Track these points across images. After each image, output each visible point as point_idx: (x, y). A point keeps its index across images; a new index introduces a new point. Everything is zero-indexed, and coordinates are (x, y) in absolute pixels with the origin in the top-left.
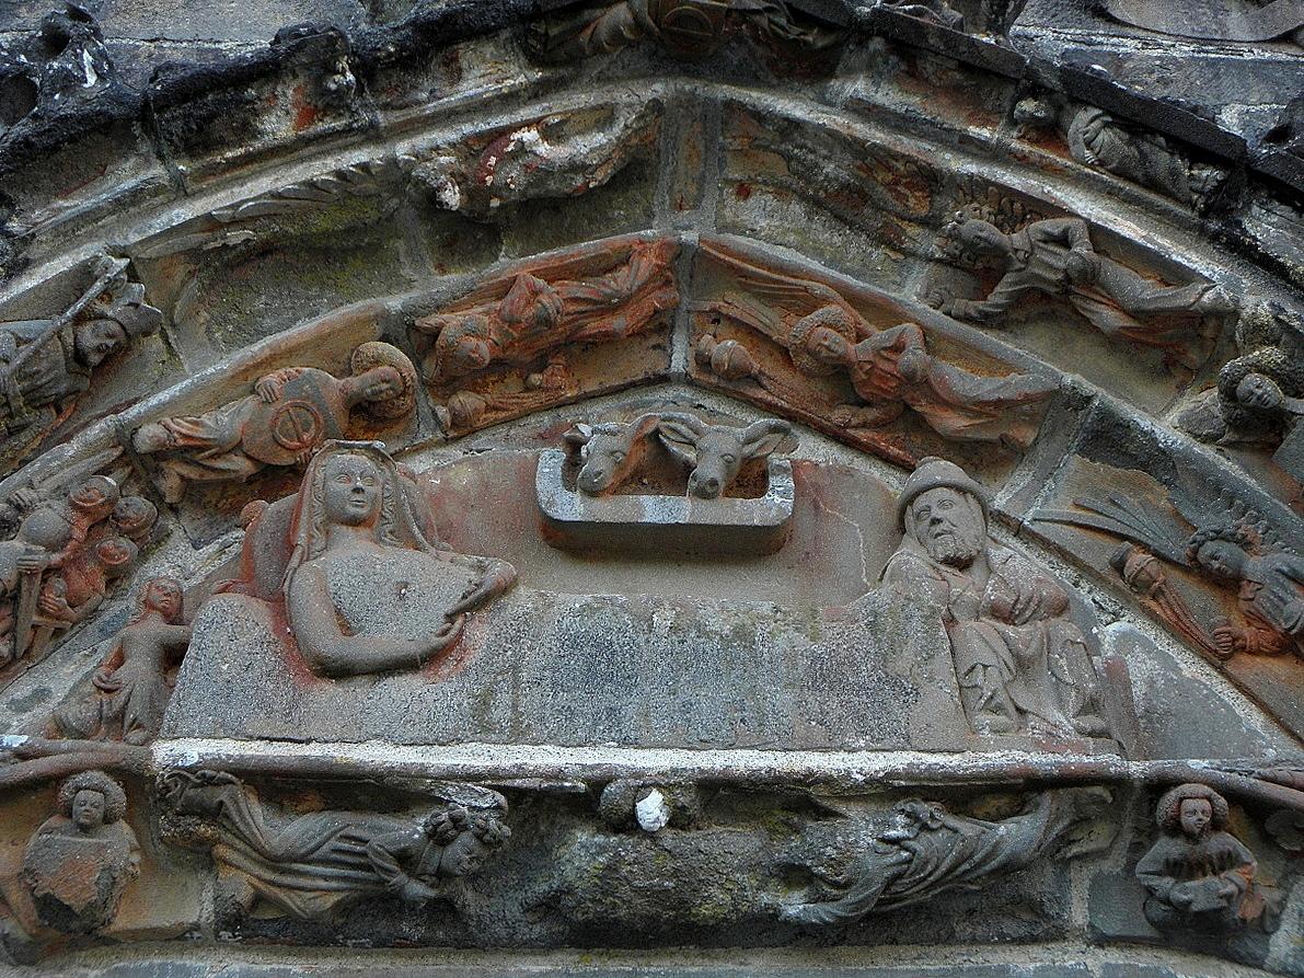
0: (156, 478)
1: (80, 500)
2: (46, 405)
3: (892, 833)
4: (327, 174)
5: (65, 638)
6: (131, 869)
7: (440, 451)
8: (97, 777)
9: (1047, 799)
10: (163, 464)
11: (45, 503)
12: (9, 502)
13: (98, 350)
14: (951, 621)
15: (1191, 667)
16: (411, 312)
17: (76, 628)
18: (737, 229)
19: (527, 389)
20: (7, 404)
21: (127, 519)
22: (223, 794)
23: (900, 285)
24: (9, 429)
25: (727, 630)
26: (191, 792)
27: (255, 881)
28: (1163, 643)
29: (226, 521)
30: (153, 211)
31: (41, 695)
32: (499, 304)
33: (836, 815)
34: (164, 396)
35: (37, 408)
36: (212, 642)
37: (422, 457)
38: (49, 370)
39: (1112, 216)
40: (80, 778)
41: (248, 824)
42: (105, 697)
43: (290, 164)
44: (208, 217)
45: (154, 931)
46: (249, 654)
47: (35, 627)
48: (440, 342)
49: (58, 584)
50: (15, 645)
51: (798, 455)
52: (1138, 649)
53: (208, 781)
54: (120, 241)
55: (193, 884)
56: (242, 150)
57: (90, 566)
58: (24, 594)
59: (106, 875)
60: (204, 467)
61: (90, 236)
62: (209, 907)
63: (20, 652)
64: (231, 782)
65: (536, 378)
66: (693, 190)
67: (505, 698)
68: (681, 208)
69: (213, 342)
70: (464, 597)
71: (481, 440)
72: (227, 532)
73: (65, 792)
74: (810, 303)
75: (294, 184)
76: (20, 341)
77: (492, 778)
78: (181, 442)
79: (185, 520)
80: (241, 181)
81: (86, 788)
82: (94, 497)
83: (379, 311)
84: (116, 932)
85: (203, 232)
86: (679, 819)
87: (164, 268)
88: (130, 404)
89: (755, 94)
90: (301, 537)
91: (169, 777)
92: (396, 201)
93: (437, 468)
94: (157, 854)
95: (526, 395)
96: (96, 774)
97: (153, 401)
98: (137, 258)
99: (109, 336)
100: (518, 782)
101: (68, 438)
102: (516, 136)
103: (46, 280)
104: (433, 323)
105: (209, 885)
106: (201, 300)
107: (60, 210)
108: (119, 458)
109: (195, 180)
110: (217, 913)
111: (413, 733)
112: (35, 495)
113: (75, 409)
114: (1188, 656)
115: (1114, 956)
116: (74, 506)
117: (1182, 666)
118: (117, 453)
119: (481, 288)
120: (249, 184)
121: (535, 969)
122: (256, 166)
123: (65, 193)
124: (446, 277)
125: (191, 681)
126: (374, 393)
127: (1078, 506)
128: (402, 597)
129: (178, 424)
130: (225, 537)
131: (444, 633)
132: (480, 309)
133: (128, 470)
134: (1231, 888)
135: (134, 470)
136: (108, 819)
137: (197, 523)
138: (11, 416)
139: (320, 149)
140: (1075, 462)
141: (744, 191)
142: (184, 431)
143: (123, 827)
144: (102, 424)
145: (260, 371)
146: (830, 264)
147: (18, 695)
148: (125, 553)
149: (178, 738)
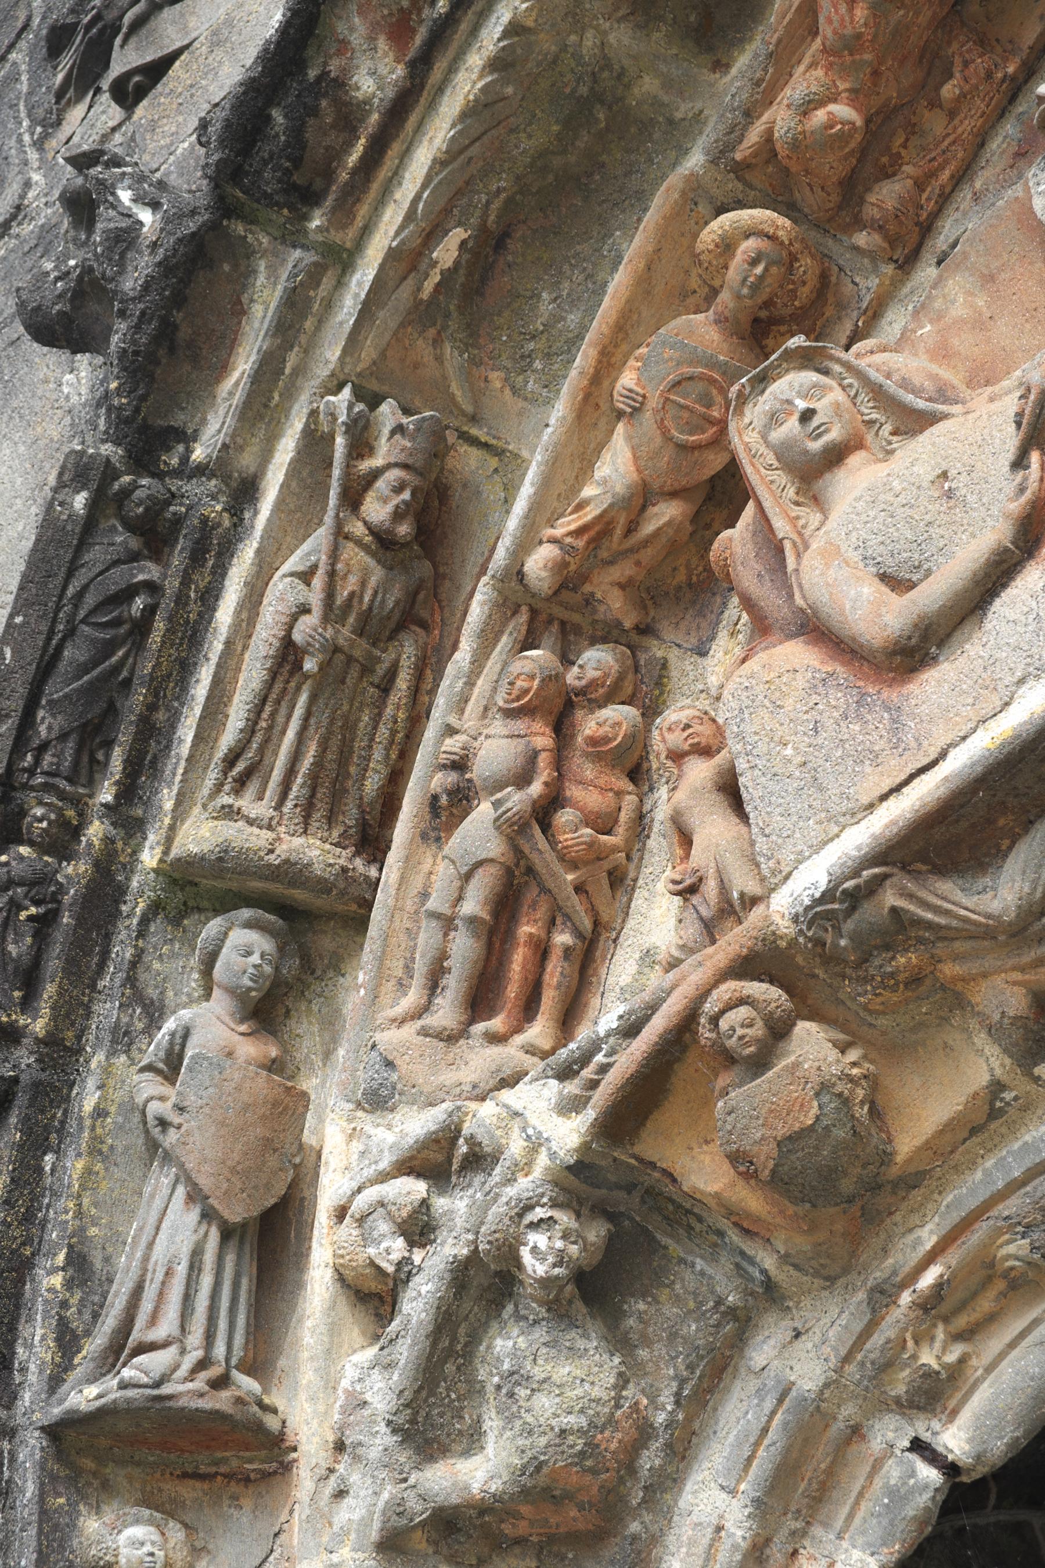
0: (595, 611)
1: (513, 701)
2: (401, 626)
4: (481, 77)
5: (632, 875)
6: (855, 1071)
7: (905, 290)
8: (729, 988)
10: (587, 588)
11: (482, 738)
12: (444, 767)
13: (398, 515)
16: (719, 155)
17: (636, 856)
19: (952, 114)
20: (350, 659)
21: (593, 684)
22: (890, 898)
24: (378, 687)
26: (849, 926)
27: (1017, 976)
29: (714, 594)
30: (329, 305)
32: (818, 43)
34: (520, 506)
35: (390, 638)
36: (756, 733)
37: (890, 315)
38: (363, 584)
40: (710, 1007)
41: (947, 913)
42: (695, 900)
43: (432, 105)
44: (392, 255)
45: (948, 1127)
46: (806, 712)
47: (579, 889)
48: (782, 150)
49: (565, 817)
50: (573, 924)
53: (855, 898)
54: (322, 372)
55: (954, 1038)
56: (363, 141)
57: (589, 771)
58: (535, 858)
59: (826, 1099)
60: (632, 550)
61: (290, 395)
62: (992, 1050)
63: (586, 924)
64: (885, 877)
65: (949, 90)
69: (533, 400)
70: (1019, 424)
71: (947, 230)
72: (725, 605)
73: (705, 1034)
75: (453, 126)
76: (306, 577)
78: (580, 543)
79: (669, 634)
80: (397, 175)
81: (722, 1012)
82: (525, 685)
83: (681, 185)
84: (909, 1161)
85: (405, 278)
87: (402, 360)
88: (493, 550)
90: (781, 526)
91: (809, 929)
92: (590, 34)
93: (916, 313)
94: (884, 1033)
95: (956, 122)
96: (723, 987)
97: (513, 523)
98: (359, 375)
99: (398, 489)
101: (455, 647)
103: (282, 486)
104: (757, 139)
105: (973, 1024)
106: (475, 362)
107: (231, 394)
108: (531, 621)
109: (344, 227)
110: (1006, 1051)
112: (461, 738)
113: (441, 608)
116: (509, 714)
118: (523, 617)
119: (779, 41)
120: (407, 175)
122: (395, 149)
123: (223, 369)
124: (734, 71)
125: (762, 798)
126: (755, 288)
129: (562, 525)
130: (726, 614)
131: (1022, 490)
132: (802, 68)
133: (555, 628)
135: (563, 623)
137: (683, 625)
138: (366, 670)
139: (450, 53)
142: (573, 527)
143: (804, 1028)
144: (478, 597)
145: (606, 383)
147: (625, 979)
148: (619, 724)
149: (790, 874)
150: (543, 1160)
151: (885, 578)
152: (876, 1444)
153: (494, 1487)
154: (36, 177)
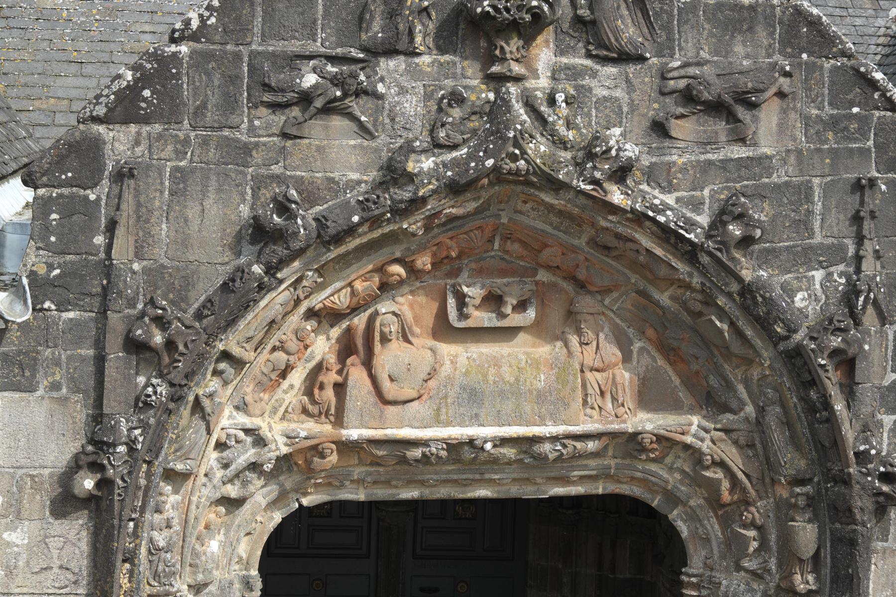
3: (557, 448)
9: (604, 438)
14: (582, 371)
15: (661, 362)
18: (521, 212)
23: (579, 238)
25: (512, 380)
28: (654, 352)
31: (292, 386)
33: (541, 443)
39: (654, 246)
44: (339, 255)
51: (538, 278)
52: (645, 354)
66: (506, 199)
67: (444, 410)
68: (501, 203)
74: (546, 246)
77: (443, 440)
86: (495, 446)
89: (532, 191)
100: (449, 441)
102: (445, 212)
111: (417, 425)
114: (661, 357)
115: (619, 461)
117: (658, 361)
121: (450, 468)
127: (632, 305)
128: (409, 370)
134: (654, 456)
136: (332, 453)
140: (634, 294)
141: (525, 202)
146: (555, 228)
150: (277, 453)
151: (389, 376)
152: (290, 495)
153: (235, 497)
154: (246, 121)
